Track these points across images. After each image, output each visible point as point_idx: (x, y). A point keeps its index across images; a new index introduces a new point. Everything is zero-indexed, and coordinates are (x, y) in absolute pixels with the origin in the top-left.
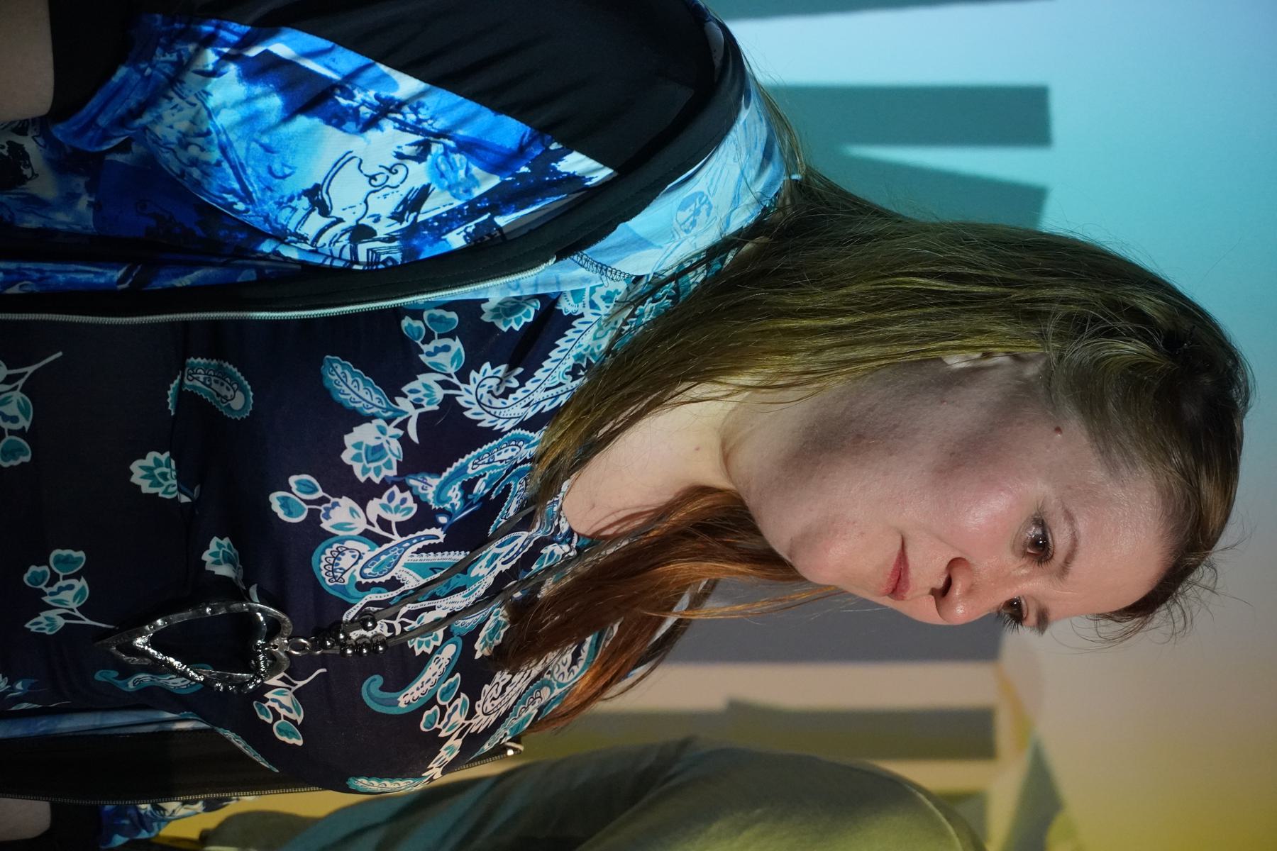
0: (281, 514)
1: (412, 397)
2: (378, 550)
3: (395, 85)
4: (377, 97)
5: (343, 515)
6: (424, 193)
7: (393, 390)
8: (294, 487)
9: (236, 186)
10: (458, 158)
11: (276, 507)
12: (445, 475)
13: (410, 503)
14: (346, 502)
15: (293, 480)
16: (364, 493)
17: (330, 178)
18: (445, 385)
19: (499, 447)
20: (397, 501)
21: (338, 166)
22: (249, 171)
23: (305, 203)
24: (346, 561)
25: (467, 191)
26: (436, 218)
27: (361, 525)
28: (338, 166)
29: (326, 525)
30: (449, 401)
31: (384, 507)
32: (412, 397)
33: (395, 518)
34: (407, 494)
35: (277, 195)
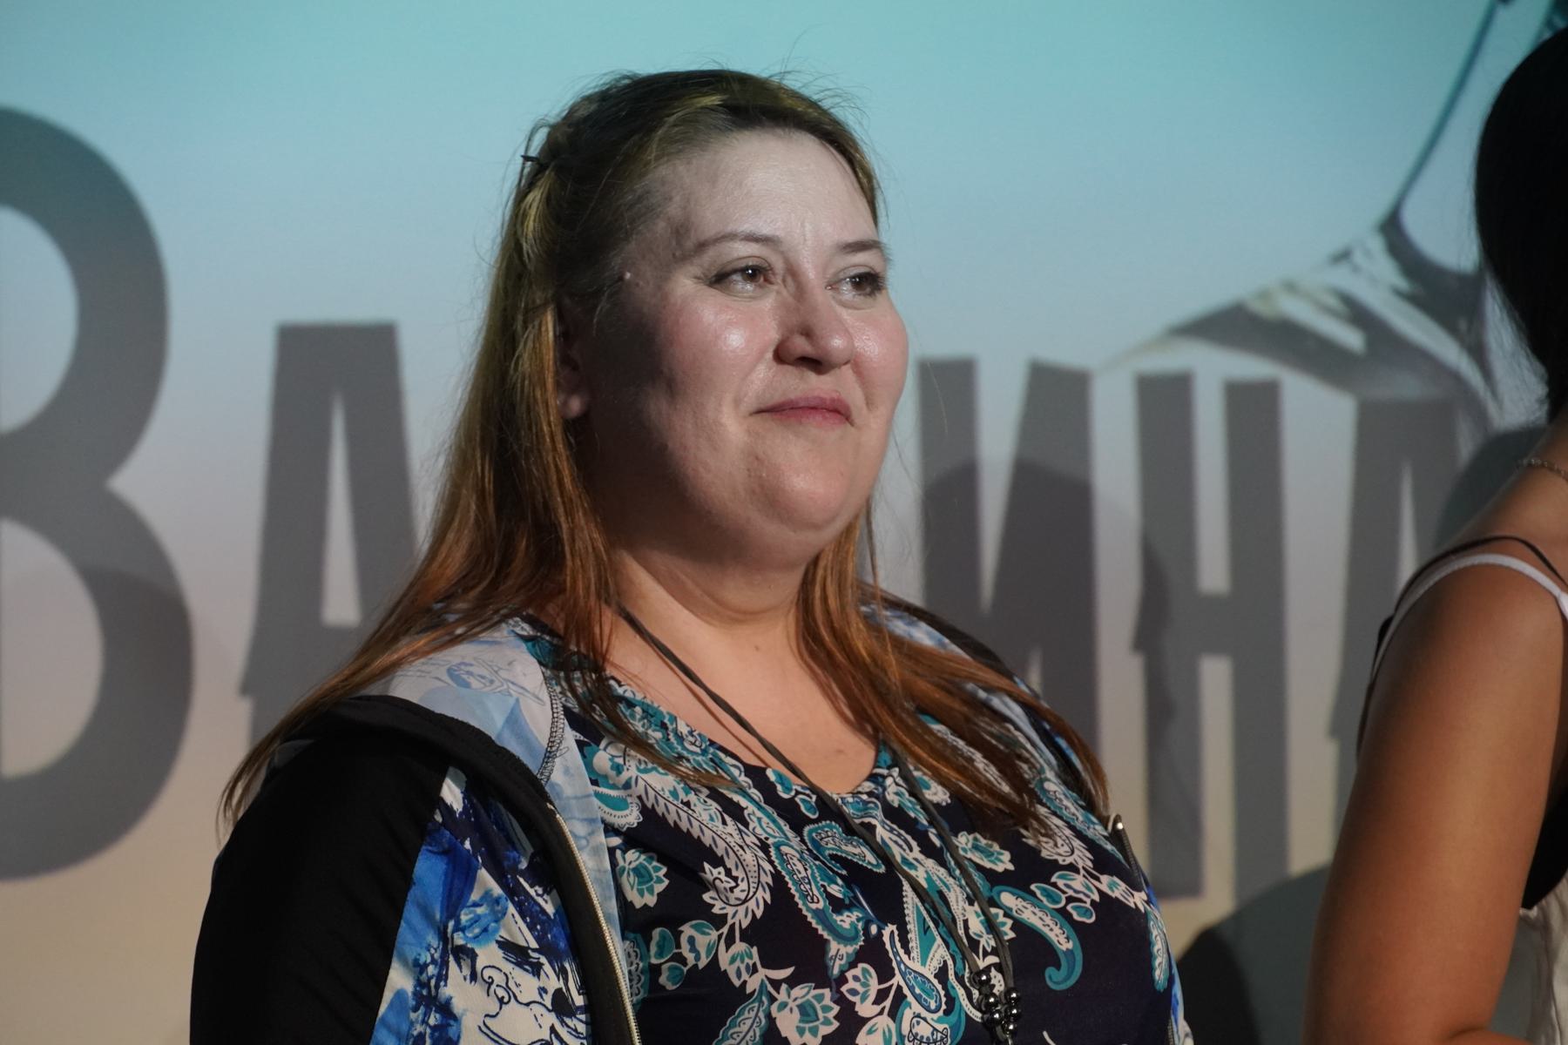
12: (826, 935)
18: (730, 941)
19: (792, 873)
30: (747, 936)
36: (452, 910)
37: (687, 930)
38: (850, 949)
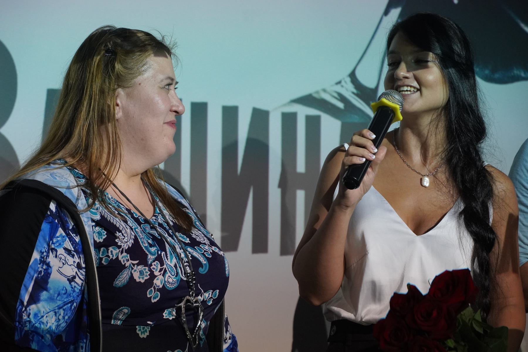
0: (158, 299)
1: (125, 262)
2: (168, 271)
3: (36, 260)
4: (40, 264)
5: (158, 282)
6: (65, 249)
7: (124, 267)
8: (151, 296)
9: (70, 305)
10: (54, 241)
11: (155, 300)
12: (147, 253)
13: (155, 263)
14: (155, 281)
15: (148, 296)
16: (153, 276)
17: (65, 276)
18: (122, 252)
19: (139, 236)
20: (155, 267)
21: (61, 274)
22: (65, 300)
23: (73, 283)
24: (170, 280)
25: (64, 237)
26: (72, 245)
27: (161, 277)
28: (61, 274)
29: (161, 287)
30: (127, 251)
31: (156, 271)
32: (125, 262)
33: (159, 267)
34: (153, 264)
35: (72, 292)
36: (51, 238)
37: (111, 249)
38: (154, 257)
